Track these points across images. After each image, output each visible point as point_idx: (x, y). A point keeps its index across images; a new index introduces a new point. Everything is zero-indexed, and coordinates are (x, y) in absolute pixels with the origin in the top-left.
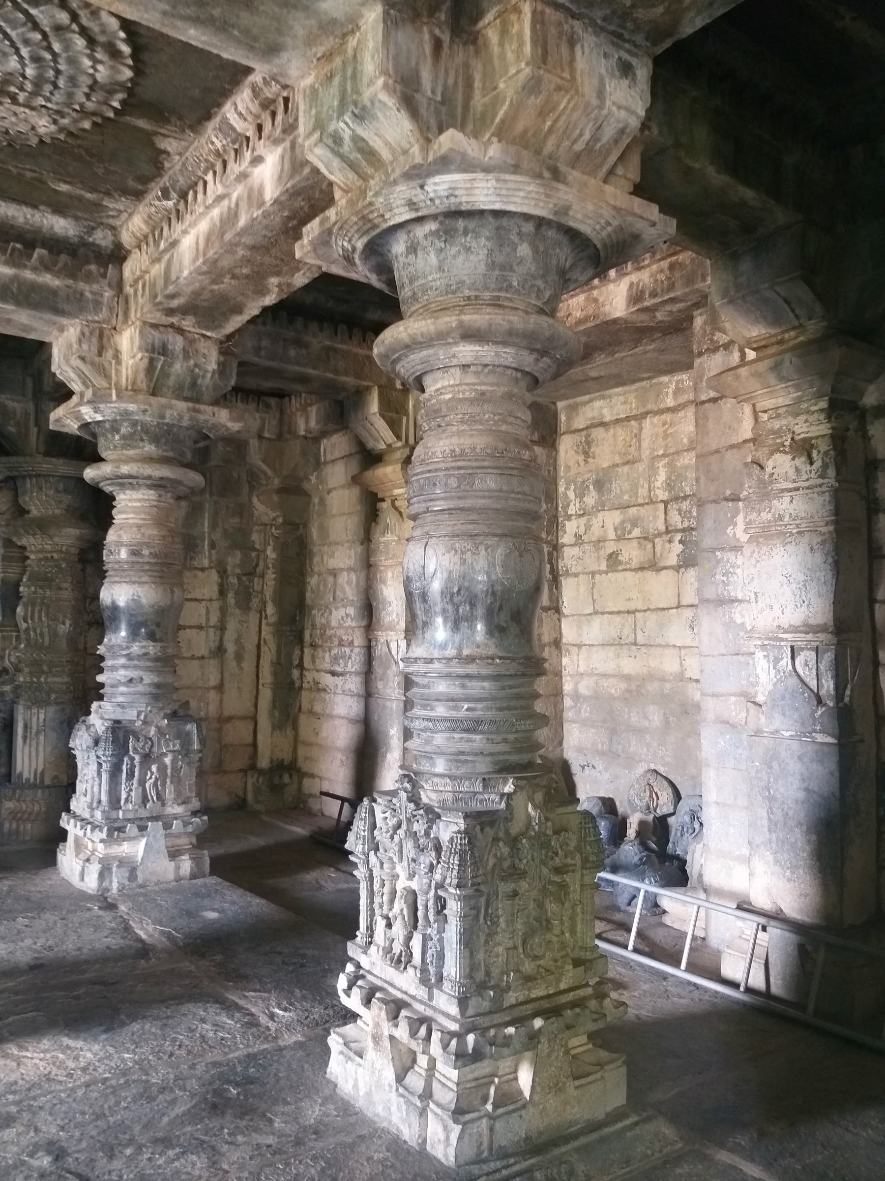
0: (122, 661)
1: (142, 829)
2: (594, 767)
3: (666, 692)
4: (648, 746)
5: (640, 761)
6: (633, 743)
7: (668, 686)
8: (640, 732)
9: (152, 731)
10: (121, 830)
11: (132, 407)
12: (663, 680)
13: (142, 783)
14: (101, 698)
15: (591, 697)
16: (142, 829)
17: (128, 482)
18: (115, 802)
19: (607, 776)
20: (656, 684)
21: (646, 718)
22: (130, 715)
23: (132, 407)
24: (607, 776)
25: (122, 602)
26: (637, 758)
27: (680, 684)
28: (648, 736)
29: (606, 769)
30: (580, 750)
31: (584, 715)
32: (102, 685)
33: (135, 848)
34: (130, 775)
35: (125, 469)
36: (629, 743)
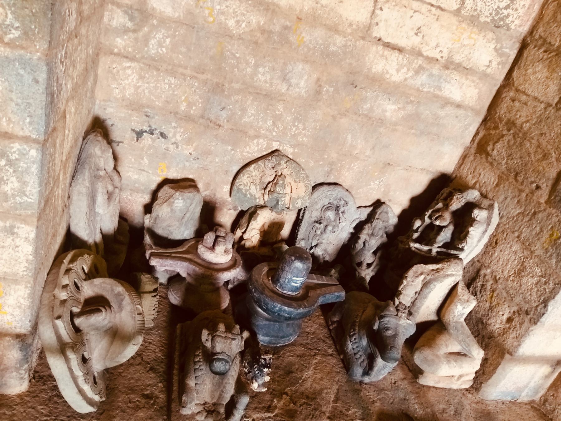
2: (162, 135)
3: (333, 48)
4: (277, 119)
5: (257, 137)
6: (251, 111)
7: (339, 40)
8: (267, 97)
12: (334, 29)
15: (178, 22)
19: (188, 150)
20: (319, 34)
21: (285, 78)
24: (188, 150)
26: (251, 133)
27: (360, 43)
28: (280, 107)
29: (189, 141)
30: (135, 106)
31: (153, 48)
36: (244, 110)
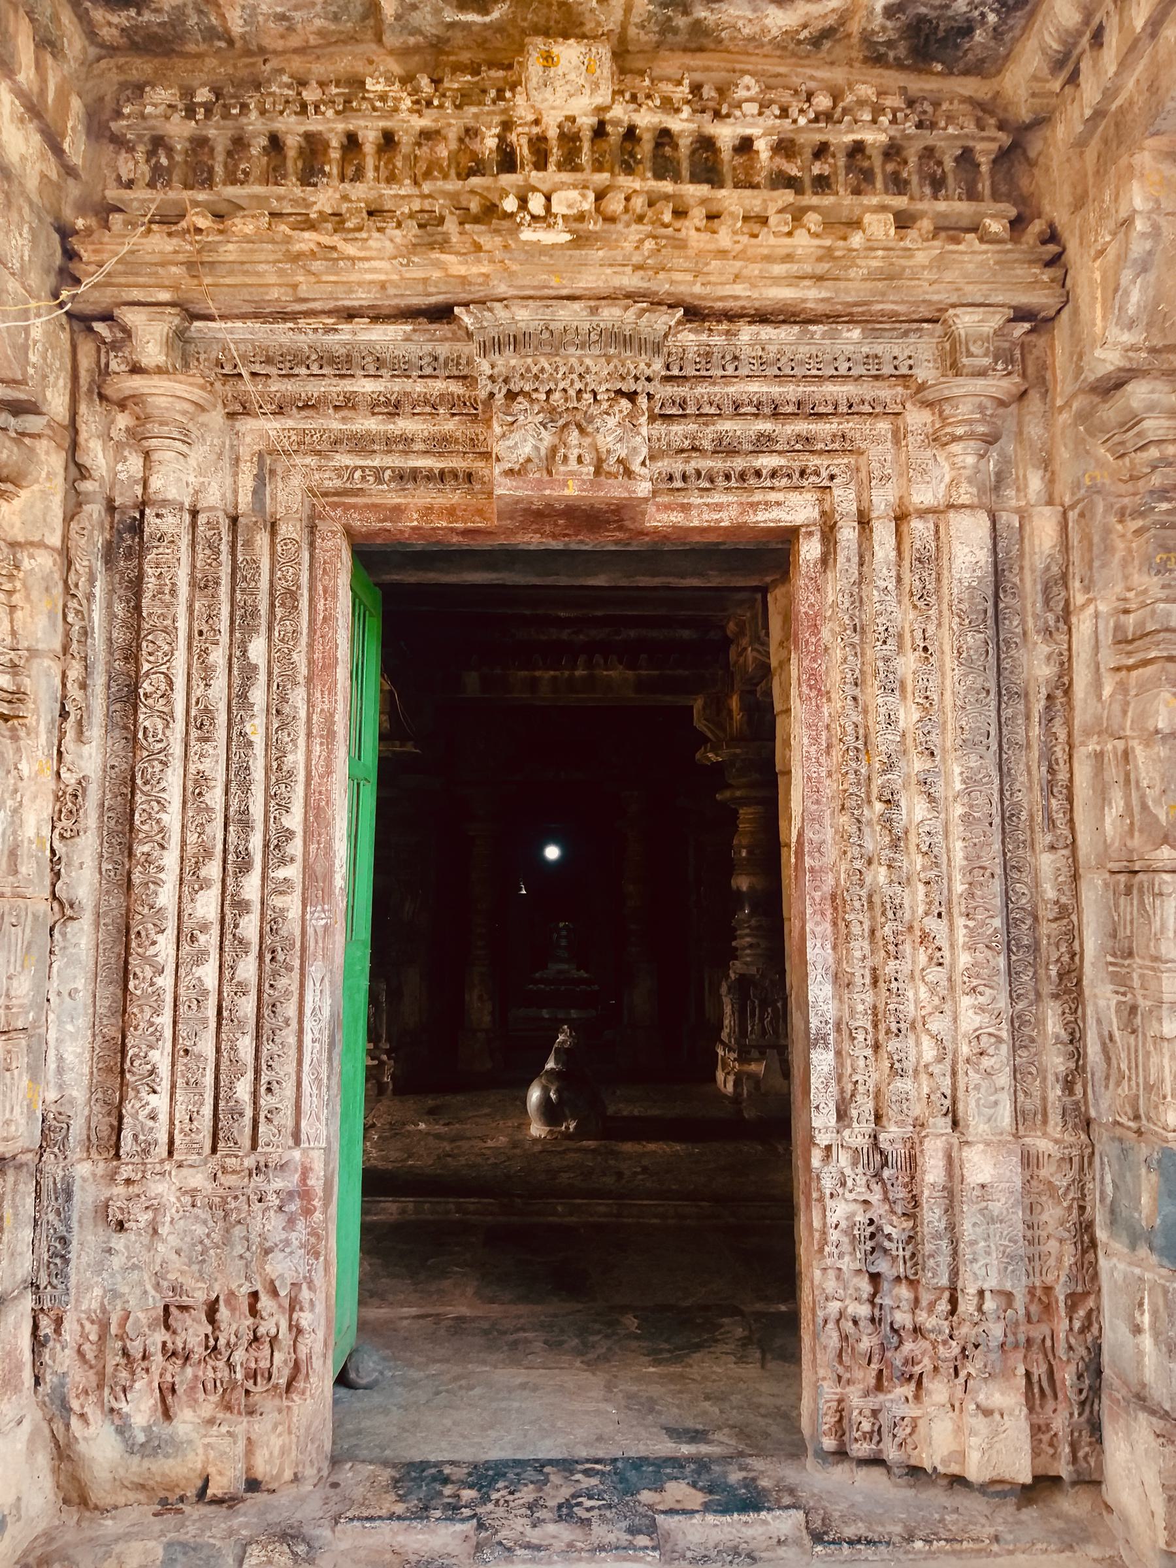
0: (747, 931)
1: (762, 1053)
9: (767, 983)
10: (749, 1052)
11: (738, 751)
13: (762, 1020)
14: (736, 958)
16: (762, 1053)
17: (745, 802)
18: (743, 1033)
22: (753, 970)
23: (738, 751)
25: (744, 888)
32: (736, 949)
33: (757, 1068)
34: (753, 1015)
35: (738, 793)
